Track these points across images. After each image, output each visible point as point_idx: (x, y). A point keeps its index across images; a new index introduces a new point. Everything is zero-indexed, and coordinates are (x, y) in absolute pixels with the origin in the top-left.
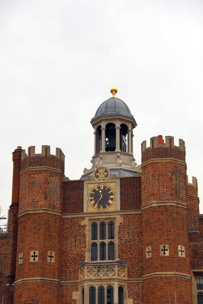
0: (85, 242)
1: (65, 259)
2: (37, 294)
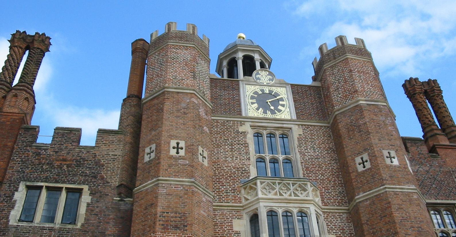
0: (247, 153)
1: (217, 172)
2: (184, 203)
